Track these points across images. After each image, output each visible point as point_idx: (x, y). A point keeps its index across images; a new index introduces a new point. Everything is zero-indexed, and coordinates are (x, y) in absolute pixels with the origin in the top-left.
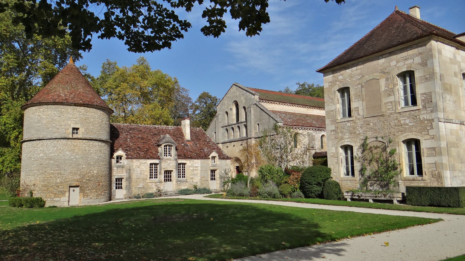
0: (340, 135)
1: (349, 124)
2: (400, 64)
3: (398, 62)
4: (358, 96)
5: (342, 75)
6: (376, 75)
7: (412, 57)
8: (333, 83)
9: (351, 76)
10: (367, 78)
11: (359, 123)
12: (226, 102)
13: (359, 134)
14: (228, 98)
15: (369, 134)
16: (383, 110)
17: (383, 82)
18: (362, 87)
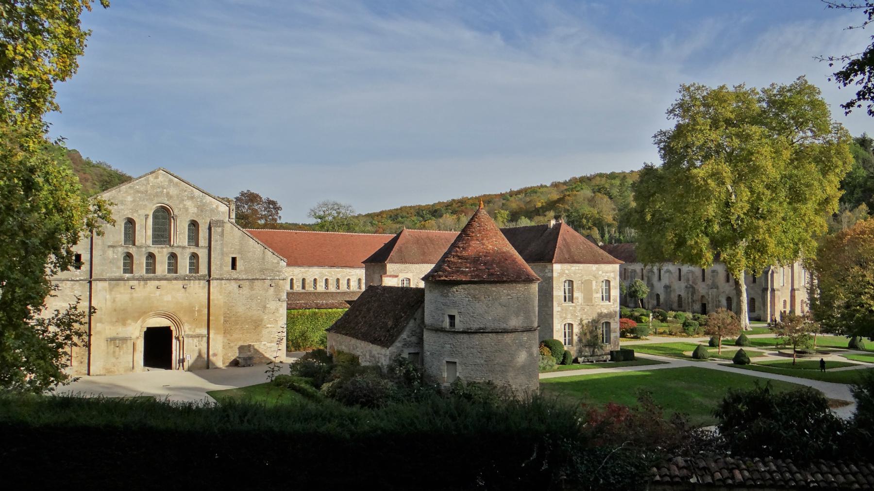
4: (578, 289)
6: (591, 278)
7: (611, 272)
8: (561, 274)
9: (575, 273)
10: (586, 278)
11: (579, 308)
12: (129, 199)
14: (138, 192)
15: (584, 317)
17: (594, 283)
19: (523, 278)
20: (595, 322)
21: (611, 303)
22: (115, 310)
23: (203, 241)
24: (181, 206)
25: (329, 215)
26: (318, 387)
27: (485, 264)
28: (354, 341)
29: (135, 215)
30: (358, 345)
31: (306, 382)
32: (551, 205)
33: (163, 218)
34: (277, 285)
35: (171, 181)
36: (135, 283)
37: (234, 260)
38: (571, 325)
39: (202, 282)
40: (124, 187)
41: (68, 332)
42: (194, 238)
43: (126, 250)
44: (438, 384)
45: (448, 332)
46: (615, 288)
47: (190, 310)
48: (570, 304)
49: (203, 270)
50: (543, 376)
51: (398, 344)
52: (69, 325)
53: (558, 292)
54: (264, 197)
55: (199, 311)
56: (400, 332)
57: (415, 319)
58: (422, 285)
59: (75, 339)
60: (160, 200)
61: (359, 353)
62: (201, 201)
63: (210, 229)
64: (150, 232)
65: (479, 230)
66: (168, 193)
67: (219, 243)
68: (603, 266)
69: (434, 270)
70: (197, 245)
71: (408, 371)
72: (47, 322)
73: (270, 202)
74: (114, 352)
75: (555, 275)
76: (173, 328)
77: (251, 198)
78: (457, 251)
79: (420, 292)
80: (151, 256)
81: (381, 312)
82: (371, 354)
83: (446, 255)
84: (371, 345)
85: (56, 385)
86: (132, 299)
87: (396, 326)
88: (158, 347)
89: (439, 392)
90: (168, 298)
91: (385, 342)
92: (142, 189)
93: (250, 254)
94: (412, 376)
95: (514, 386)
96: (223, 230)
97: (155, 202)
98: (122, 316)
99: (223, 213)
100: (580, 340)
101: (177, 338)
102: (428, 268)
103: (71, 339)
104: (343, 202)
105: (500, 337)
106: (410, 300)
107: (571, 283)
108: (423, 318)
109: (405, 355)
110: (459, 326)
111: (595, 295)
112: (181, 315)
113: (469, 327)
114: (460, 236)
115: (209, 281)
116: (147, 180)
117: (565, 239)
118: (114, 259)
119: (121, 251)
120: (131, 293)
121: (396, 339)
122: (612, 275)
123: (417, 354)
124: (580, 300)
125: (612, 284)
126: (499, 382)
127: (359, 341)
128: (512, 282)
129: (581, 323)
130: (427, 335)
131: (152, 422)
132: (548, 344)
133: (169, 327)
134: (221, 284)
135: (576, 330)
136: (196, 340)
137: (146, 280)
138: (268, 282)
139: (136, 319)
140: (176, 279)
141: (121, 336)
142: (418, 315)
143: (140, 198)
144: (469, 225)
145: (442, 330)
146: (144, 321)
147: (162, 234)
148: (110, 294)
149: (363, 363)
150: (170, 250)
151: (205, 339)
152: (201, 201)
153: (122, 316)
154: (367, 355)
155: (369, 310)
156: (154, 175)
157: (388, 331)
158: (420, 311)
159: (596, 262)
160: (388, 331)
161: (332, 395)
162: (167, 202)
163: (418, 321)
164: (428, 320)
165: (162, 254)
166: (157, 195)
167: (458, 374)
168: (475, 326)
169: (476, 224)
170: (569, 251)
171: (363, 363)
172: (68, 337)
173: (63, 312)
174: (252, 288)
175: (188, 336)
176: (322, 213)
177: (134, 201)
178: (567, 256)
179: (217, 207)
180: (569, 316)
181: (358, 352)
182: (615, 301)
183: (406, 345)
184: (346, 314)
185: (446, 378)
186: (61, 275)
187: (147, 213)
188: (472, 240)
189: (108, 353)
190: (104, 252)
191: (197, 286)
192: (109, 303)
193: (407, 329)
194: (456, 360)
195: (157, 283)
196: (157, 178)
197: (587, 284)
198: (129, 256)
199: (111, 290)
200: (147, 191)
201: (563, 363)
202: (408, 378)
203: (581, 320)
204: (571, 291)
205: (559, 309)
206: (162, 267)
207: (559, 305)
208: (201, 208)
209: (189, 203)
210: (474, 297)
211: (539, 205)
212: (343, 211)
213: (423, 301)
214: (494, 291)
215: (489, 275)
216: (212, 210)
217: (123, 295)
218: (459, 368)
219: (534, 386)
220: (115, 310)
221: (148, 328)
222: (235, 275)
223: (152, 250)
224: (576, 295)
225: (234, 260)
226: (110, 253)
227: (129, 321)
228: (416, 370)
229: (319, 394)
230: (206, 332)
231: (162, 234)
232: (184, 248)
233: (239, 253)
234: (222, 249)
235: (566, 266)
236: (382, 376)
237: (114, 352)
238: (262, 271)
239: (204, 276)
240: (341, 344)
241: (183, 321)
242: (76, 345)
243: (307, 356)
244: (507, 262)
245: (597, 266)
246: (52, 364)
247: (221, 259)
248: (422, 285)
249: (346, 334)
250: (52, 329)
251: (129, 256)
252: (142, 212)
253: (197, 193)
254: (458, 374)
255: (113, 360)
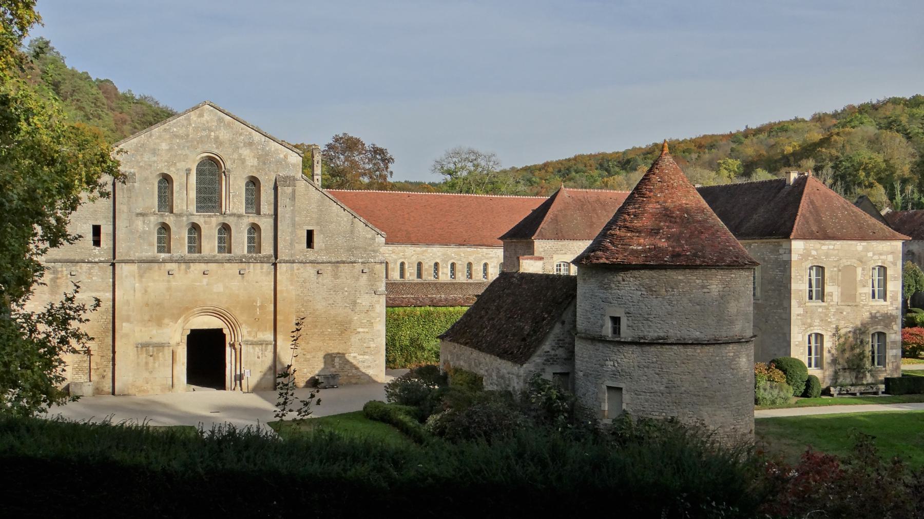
0: (809, 321)
1: (820, 310)
2: (876, 257)
3: (874, 254)
5: (816, 250)
6: (854, 262)
8: (805, 256)
10: (845, 262)
11: (833, 310)
12: (164, 146)
13: (830, 322)
14: (176, 136)
15: (842, 324)
16: (858, 300)
17: (859, 270)
18: (839, 270)
19: (728, 260)
20: (860, 332)
21: (888, 303)
22: (147, 305)
23: (266, 207)
24: (236, 156)
25: (462, 168)
26: (423, 420)
27: (668, 239)
28: (476, 354)
29: (172, 169)
30: (482, 360)
31: (408, 413)
32: (809, 150)
33: (211, 171)
34: (372, 271)
35: (220, 120)
36: (173, 266)
37: (310, 234)
38: (819, 337)
39: (266, 266)
40: (156, 130)
41: (63, 333)
42: (254, 203)
43: (161, 220)
44: (595, 421)
45: (610, 342)
46: (895, 279)
47: (249, 306)
48: (820, 303)
49: (267, 249)
50: (761, 413)
51: (537, 359)
52: (64, 322)
53: (799, 285)
54: (368, 145)
55: (262, 307)
56: (540, 342)
57: (563, 323)
58: (574, 270)
59: (73, 342)
60: (207, 147)
61: (482, 372)
62: (263, 149)
63: (276, 188)
64: (193, 194)
65: (661, 188)
66: (217, 138)
67: (289, 209)
68: (874, 244)
69: (591, 249)
70: (258, 213)
71: (549, 399)
72: (34, 318)
73: (377, 151)
74: (147, 363)
75: (794, 257)
76: (226, 331)
77: (350, 145)
78: (625, 220)
79: (570, 282)
80: (195, 228)
81: (517, 312)
82: (500, 374)
83: (609, 227)
84: (499, 361)
85: (49, 405)
86: (169, 289)
87: (535, 332)
88: (207, 357)
89: (595, 432)
90: (219, 288)
91: (518, 356)
92: (182, 132)
93: (333, 226)
94: (558, 407)
95: (711, 427)
96: (294, 191)
97: (199, 150)
98: (158, 313)
99: (294, 165)
100: (834, 361)
101: (232, 346)
102: (581, 247)
103: (68, 343)
104: (482, 149)
105: (690, 350)
106: (557, 292)
107: (821, 270)
108: (575, 321)
109: (548, 376)
110: (626, 333)
111: (861, 290)
112: (237, 313)
113: (641, 334)
114: (630, 200)
115: (275, 265)
116: (188, 119)
117: (812, 202)
118: (144, 232)
119: (154, 220)
120: (169, 281)
121: (534, 352)
122: (890, 258)
123: (565, 375)
124: (836, 298)
125: (889, 272)
126: (687, 419)
127: (482, 355)
128: (714, 266)
129: (836, 333)
130: (580, 347)
131: (117, 456)
132: (784, 366)
133: (221, 330)
134: (292, 269)
135: (828, 343)
136: (257, 349)
137: (188, 262)
138: (358, 267)
139: (175, 318)
140: (229, 261)
141: (155, 340)
142: (567, 316)
143: (179, 146)
144: (646, 179)
145: (600, 340)
146: (186, 321)
147: (209, 198)
148: (141, 281)
149: (489, 386)
150: (221, 219)
151: (271, 348)
152: (263, 149)
153: (158, 313)
154: (494, 374)
155: (498, 308)
156: (197, 111)
157: (524, 340)
158: (571, 308)
159: (863, 238)
160: (524, 340)
161: (441, 431)
162: (216, 151)
163: (567, 327)
164: (581, 325)
165: (210, 225)
166: (201, 141)
167: (624, 407)
168: (652, 334)
169: (655, 178)
170: (818, 221)
171: (488, 387)
172: (63, 341)
173: (57, 305)
174: (336, 276)
175: (247, 343)
176: (452, 166)
177: (170, 149)
178: (814, 229)
179: (286, 157)
180: (817, 322)
181: (482, 372)
182: (894, 299)
183: (550, 360)
184: (467, 314)
185: (606, 411)
186: (53, 253)
187: (188, 166)
188: (649, 202)
189: (138, 364)
190: (131, 222)
191: (258, 271)
192: (138, 295)
193: (552, 337)
194: (621, 385)
195: (203, 266)
196: (201, 115)
197: (848, 272)
198: (164, 228)
199: (141, 276)
200: (188, 136)
201: (805, 394)
202: (550, 411)
203: (837, 329)
204: (821, 283)
205: (801, 311)
206: (210, 245)
207: (800, 305)
208: (264, 158)
209: (246, 152)
210: (650, 289)
211: (789, 149)
212: (483, 163)
213: (574, 297)
214: (681, 281)
215: (673, 256)
216: (279, 162)
217: (157, 283)
218: (626, 397)
219: (746, 427)
220: (147, 305)
221: (192, 331)
222: (311, 255)
223: (196, 220)
224: (828, 289)
225: (310, 234)
226: (139, 223)
227: (166, 321)
228: (562, 398)
229: (424, 429)
230: (272, 338)
231: (209, 198)
232: (240, 216)
233: (318, 224)
234: (293, 219)
235: (813, 244)
236: (512, 406)
237: (147, 363)
238: (350, 250)
239: (269, 257)
240: (458, 359)
241: (240, 320)
242: (74, 351)
243: (408, 376)
244: (703, 237)
245: (864, 243)
246: (43, 377)
247: (292, 233)
248: (574, 270)
249: (466, 344)
250: (42, 327)
251: (164, 228)
252: (182, 165)
253: (257, 137)
254: (624, 407)
255: (146, 374)
